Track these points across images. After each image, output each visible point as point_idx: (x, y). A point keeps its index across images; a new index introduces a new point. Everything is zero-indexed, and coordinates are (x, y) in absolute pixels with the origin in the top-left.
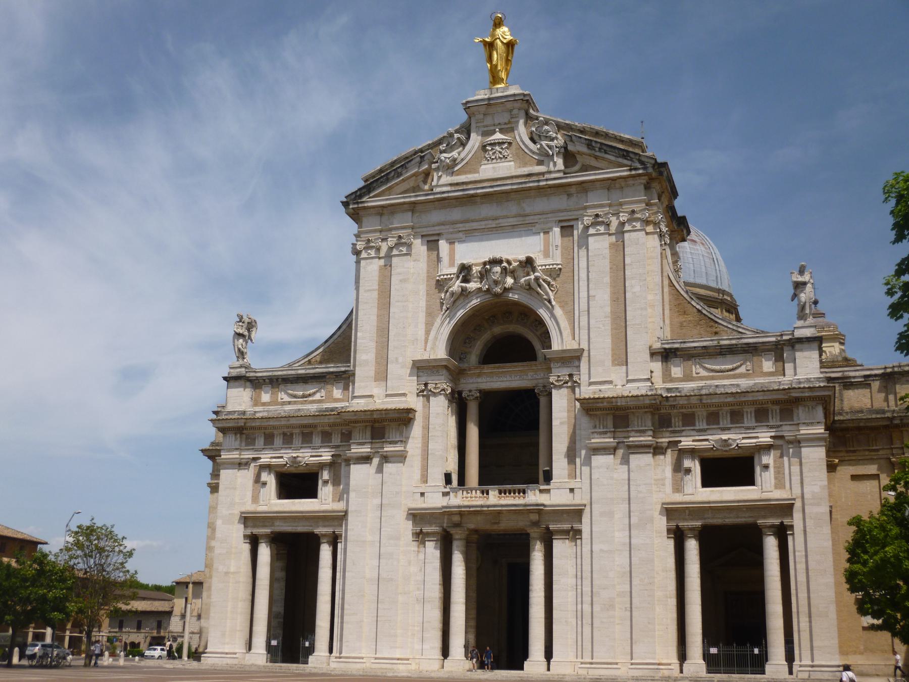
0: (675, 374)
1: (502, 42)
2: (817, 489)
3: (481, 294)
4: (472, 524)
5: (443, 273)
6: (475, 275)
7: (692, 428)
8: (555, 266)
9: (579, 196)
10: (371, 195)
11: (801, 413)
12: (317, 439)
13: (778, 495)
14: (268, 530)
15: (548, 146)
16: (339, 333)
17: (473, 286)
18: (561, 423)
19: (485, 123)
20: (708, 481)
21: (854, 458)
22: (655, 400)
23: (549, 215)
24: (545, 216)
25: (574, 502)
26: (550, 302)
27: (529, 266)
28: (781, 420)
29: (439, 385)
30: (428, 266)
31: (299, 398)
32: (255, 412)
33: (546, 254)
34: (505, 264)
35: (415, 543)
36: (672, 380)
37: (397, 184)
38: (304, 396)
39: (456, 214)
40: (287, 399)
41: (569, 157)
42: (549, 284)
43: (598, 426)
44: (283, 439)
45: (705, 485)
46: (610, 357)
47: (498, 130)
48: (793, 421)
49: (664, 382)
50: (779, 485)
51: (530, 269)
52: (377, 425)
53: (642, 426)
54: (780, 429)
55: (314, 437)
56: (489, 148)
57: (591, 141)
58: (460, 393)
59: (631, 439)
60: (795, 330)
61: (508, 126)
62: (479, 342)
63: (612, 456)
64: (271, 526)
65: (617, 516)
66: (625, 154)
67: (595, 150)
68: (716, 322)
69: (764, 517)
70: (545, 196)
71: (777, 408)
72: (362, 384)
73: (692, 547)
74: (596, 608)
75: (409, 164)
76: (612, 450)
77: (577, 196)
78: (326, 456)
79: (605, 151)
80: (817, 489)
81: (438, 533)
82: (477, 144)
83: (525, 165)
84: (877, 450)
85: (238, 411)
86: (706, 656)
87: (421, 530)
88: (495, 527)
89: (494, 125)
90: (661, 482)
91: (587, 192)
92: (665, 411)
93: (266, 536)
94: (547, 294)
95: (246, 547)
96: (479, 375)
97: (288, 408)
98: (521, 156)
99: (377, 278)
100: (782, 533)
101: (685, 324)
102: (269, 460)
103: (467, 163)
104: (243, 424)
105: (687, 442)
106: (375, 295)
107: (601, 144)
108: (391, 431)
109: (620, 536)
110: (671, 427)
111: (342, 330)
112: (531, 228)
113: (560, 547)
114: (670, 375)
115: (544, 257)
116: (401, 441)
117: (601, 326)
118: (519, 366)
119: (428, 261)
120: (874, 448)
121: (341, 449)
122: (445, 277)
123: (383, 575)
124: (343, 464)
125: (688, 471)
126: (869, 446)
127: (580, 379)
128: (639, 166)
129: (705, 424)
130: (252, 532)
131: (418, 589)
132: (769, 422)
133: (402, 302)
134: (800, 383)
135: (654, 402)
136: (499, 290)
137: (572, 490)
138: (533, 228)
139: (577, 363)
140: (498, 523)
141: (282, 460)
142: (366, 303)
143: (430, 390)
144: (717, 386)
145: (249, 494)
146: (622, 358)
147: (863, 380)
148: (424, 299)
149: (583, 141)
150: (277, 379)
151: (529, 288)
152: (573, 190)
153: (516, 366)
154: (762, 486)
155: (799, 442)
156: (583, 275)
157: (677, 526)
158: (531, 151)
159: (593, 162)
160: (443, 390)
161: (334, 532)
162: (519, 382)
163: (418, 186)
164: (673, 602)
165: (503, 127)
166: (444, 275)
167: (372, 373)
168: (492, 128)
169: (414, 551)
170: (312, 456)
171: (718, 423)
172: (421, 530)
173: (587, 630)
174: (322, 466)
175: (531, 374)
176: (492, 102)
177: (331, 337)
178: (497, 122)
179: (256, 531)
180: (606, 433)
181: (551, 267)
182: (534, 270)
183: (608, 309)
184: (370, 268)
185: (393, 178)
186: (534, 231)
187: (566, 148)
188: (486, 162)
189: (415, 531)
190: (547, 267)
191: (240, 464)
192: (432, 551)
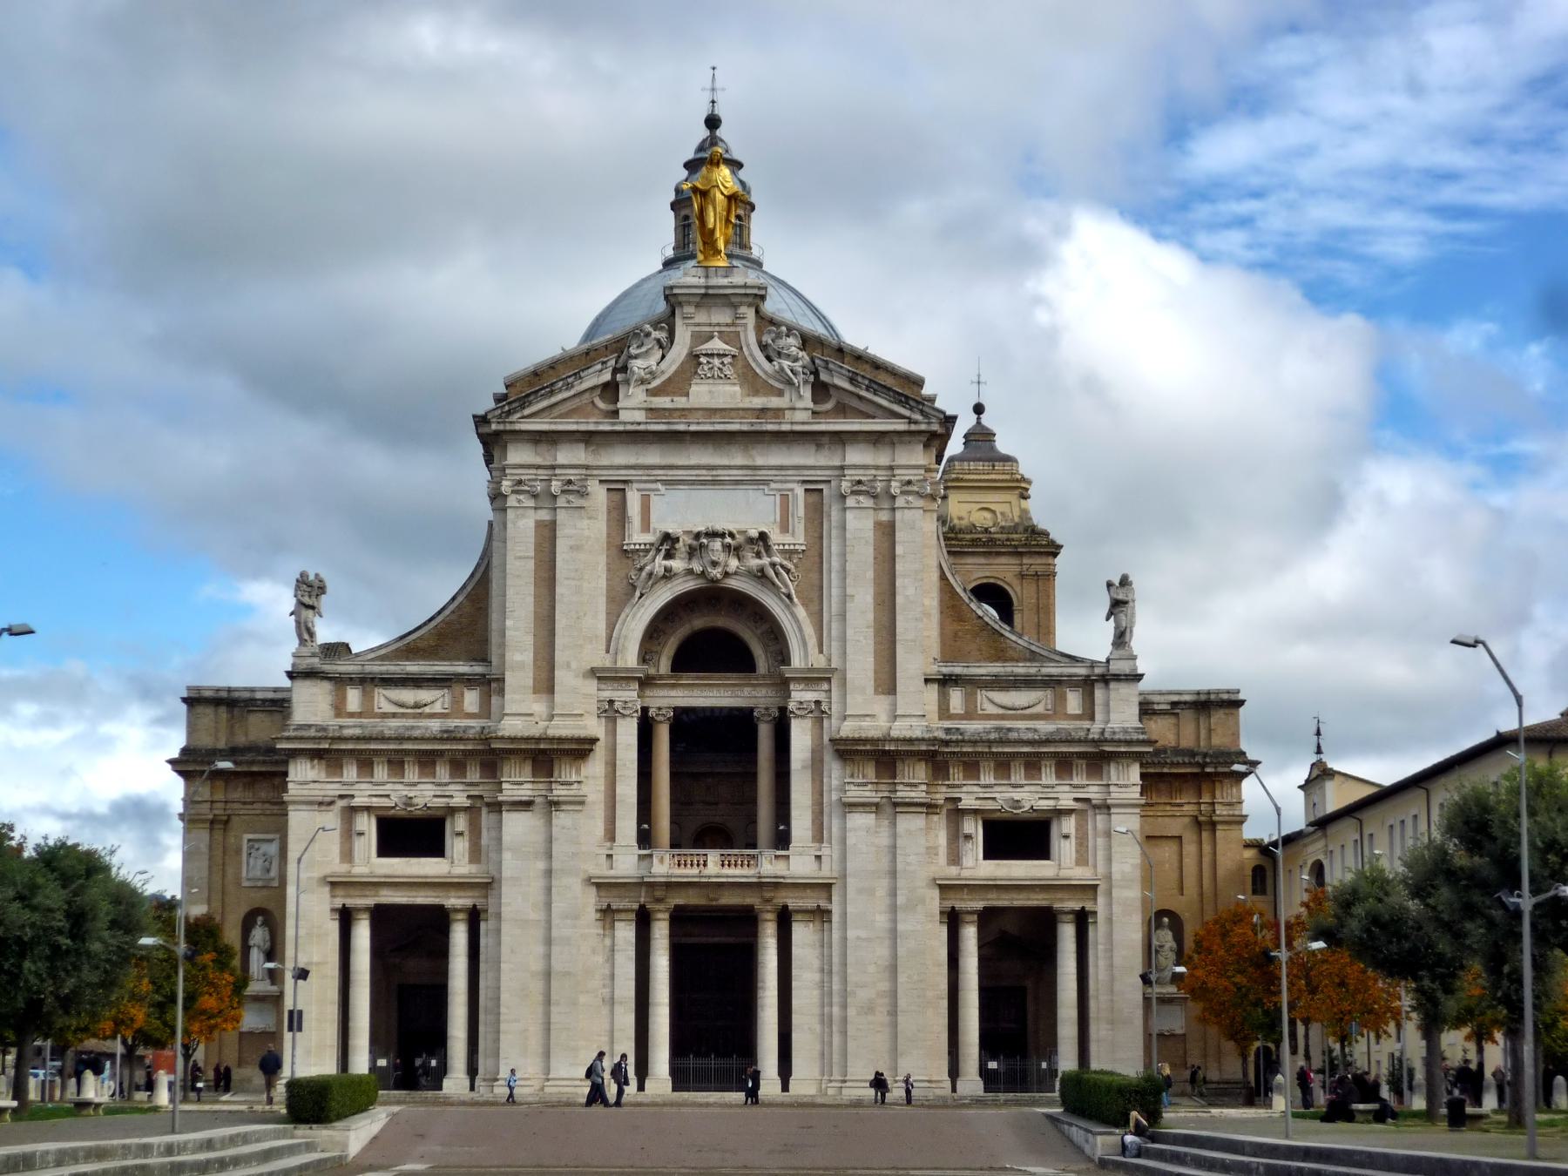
0: (954, 708)
1: (722, 193)
2: (1127, 868)
3: (689, 577)
4: (679, 900)
5: (634, 541)
6: (683, 549)
7: (975, 782)
8: (797, 547)
9: (833, 448)
10: (527, 412)
11: (1114, 773)
12: (443, 771)
13: (1080, 874)
14: (371, 901)
15: (792, 371)
16: (452, 607)
17: (677, 564)
18: (804, 767)
19: (697, 320)
20: (994, 850)
21: (1151, 813)
22: (934, 745)
23: (790, 472)
24: (783, 473)
25: (822, 874)
26: (789, 596)
27: (761, 543)
28: (1088, 779)
29: (630, 705)
30: (609, 527)
31: (407, 708)
32: (341, 727)
33: (785, 528)
34: (728, 540)
35: (600, 924)
36: (950, 717)
37: (565, 400)
38: (417, 706)
39: (652, 456)
40: (389, 708)
41: (821, 390)
42: (788, 571)
43: (856, 775)
44: (389, 770)
45: (987, 856)
46: (872, 682)
47: (716, 334)
48: (1102, 780)
49: (940, 719)
50: (1082, 860)
51: (763, 551)
52: (540, 758)
53: (914, 778)
54: (1085, 790)
55: (438, 769)
56: (703, 360)
57: (857, 374)
58: (645, 710)
59: (899, 794)
60: (1111, 662)
61: (732, 329)
62: (672, 639)
63: (873, 816)
64: (375, 896)
65: (878, 894)
66: (904, 400)
67: (860, 387)
68: (1002, 635)
69: (1062, 900)
70: (784, 442)
71: (1083, 763)
72: (516, 697)
73: (970, 935)
74: (851, 1012)
75: (586, 373)
76: (874, 809)
77: (830, 448)
78: (460, 799)
79: (875, 390)
80: (1127, 868)
81: (632, 910)
82: (685, 352)
83: (755, 392)
84: (1181, 805)
85: (316, 725)
86: (984, 1072)
87: (609, 906)
88: (714, 903)
89: (710, 325)
90: (931, 851)
91: (844, 444)
92: (941, 758)
93: (367, 909)
94: (786, 586)
95: (333, 928)
96: (673, 686)
97: (394, 723)
98: (752, 382)
99: (533, 540)
100: (1082, 920)
101: (960, 634)
102: (366, 799)
103: (670, 379)
104: (327, 746)
105: (968, 802)
106: (531, 565)
107: (870, 380)
108: (563, 767)
109: (882, 920)
110: (949, 780)
111: (456, 603)
112: (761, 487)
113: (802, 934)
114: (948, 710)
115: (781, 532)
116: (579, 782)
117: (861, 638)
118: (733, 678)
119: (608, 520)
120: (1178, 801)
121: (481, 788)
122: (637, 547)
123: (557, 965)
124: (484, 811)
125: (968, 837)
126: (1172, 798)
127: (830, 709)
128: (918, 417)
129: (992, 779)
130: (344, 905)
131: (604, 986)
132: (1072, 779)
133: (573, 579)
134: (1114, 733)
135: (933, 748)
136: (718, 575)
137: (818, 858)
138: (766, 487)
139: (825, 686)
140: (717, 900)
141: (386, 800)
142: (518, 576)
143: (617, 711)
144: (1009, 730)
145: (335, 849)
146: (888, 683)
147: (1169, 707)
148: (604, 576)
149: (844, 372)
150: (372, 679)
151: (761, 576)
152: (825, 439)
153: (729, 679)
154: (1060, 860)
155: (1108, 807)
156: (835, 564)
157: (953, 908)
158: (766, 372)
159: (855, 403)
160: (637, 711)
161: (475, 906)
162: (732, 700)
163: (593, 402)
164: (945, 1003)
165: (723, 329)
166: (635, 544)
167: (531, 682)
168: (710, 329)
169: (598, 935)
170: (435, 796)
171: (1009, 778)
172: (609, 906)
173: (836, 1039)
174: (452, 811)
175: (749, 689)
176: (711, 291)
177: (439, 613)
178: (714, 321)
179: (350, 902)
180: (865, 784)
181: (792, 547)
182: (768, 548)
183: (871, 616)
184: (522, 523)
185: (560, 390)
186: (766, 492)
187: (816, 373)
188: (699, 381)
189: (599, 907)
190: (787, 547)
191: (321, 804)
192: (626, 933)
